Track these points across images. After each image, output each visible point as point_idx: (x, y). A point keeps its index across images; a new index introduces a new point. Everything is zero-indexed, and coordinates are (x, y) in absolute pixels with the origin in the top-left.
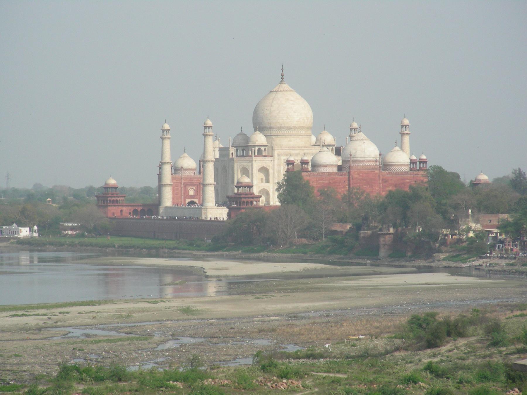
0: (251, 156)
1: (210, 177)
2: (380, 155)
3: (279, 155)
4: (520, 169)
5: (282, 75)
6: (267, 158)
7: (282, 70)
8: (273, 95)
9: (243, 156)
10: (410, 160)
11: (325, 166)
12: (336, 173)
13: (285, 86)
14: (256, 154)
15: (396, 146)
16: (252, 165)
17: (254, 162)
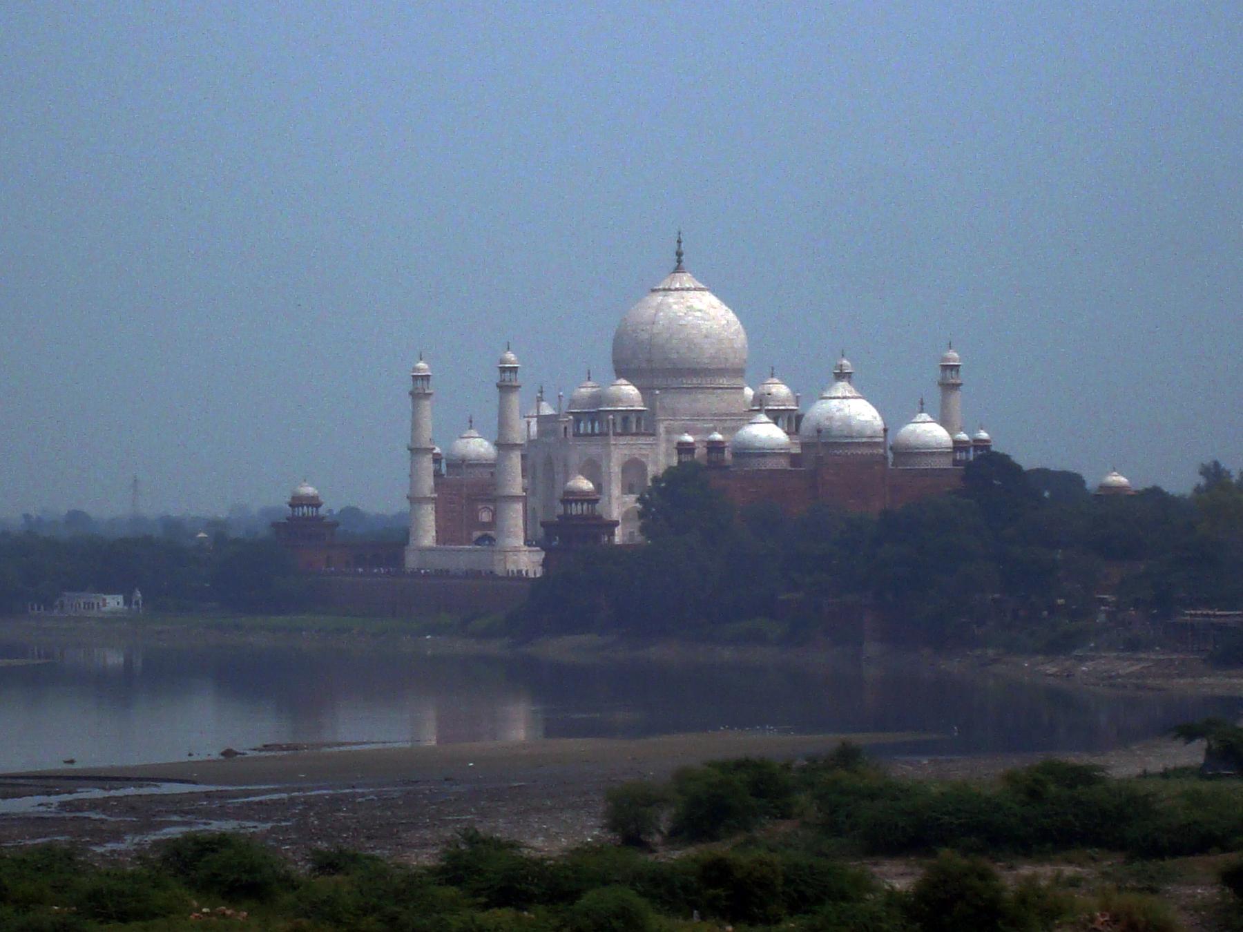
0: (607, 434)
1: (516, 485)
2: (885, 430)
3: (669, 431)
4: (1216, 464)
5: (679, 254)
6: (642, 440)
7: (679, 242)
8: (659, 298)
9: (593, 434)
10: (955, 442)
11: (764, 455)
12: (784, 471)
13: (686, 280)
14: (619, 431)
15: (922, 411)
16: (609, 455)
17: (613, 448)
